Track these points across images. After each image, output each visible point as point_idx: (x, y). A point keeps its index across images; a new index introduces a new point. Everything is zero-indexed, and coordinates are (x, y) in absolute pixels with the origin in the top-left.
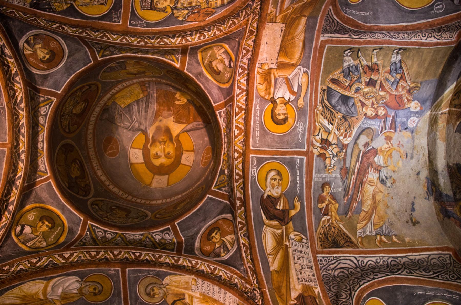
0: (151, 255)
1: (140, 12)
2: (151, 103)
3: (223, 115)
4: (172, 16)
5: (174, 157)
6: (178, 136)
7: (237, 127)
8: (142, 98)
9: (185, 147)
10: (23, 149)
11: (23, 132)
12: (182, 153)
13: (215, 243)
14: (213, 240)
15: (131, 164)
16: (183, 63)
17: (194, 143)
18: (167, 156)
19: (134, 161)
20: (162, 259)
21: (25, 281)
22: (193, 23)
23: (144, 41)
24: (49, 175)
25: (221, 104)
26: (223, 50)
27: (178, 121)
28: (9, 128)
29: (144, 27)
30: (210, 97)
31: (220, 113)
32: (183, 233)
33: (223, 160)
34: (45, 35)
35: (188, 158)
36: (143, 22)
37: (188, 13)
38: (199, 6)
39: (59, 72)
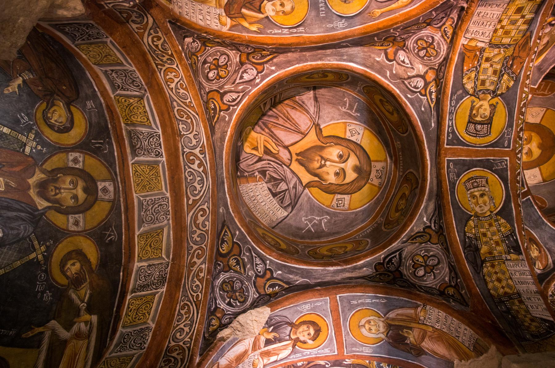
4: (503, 96)
5: (530, 132)
15: (544, 181)
19: (539, 178)
22: (525, 65)
29: (512, 130)
35: (534, 114)
36: (506, 131)
37: (508, 74)
39: (540, 235)
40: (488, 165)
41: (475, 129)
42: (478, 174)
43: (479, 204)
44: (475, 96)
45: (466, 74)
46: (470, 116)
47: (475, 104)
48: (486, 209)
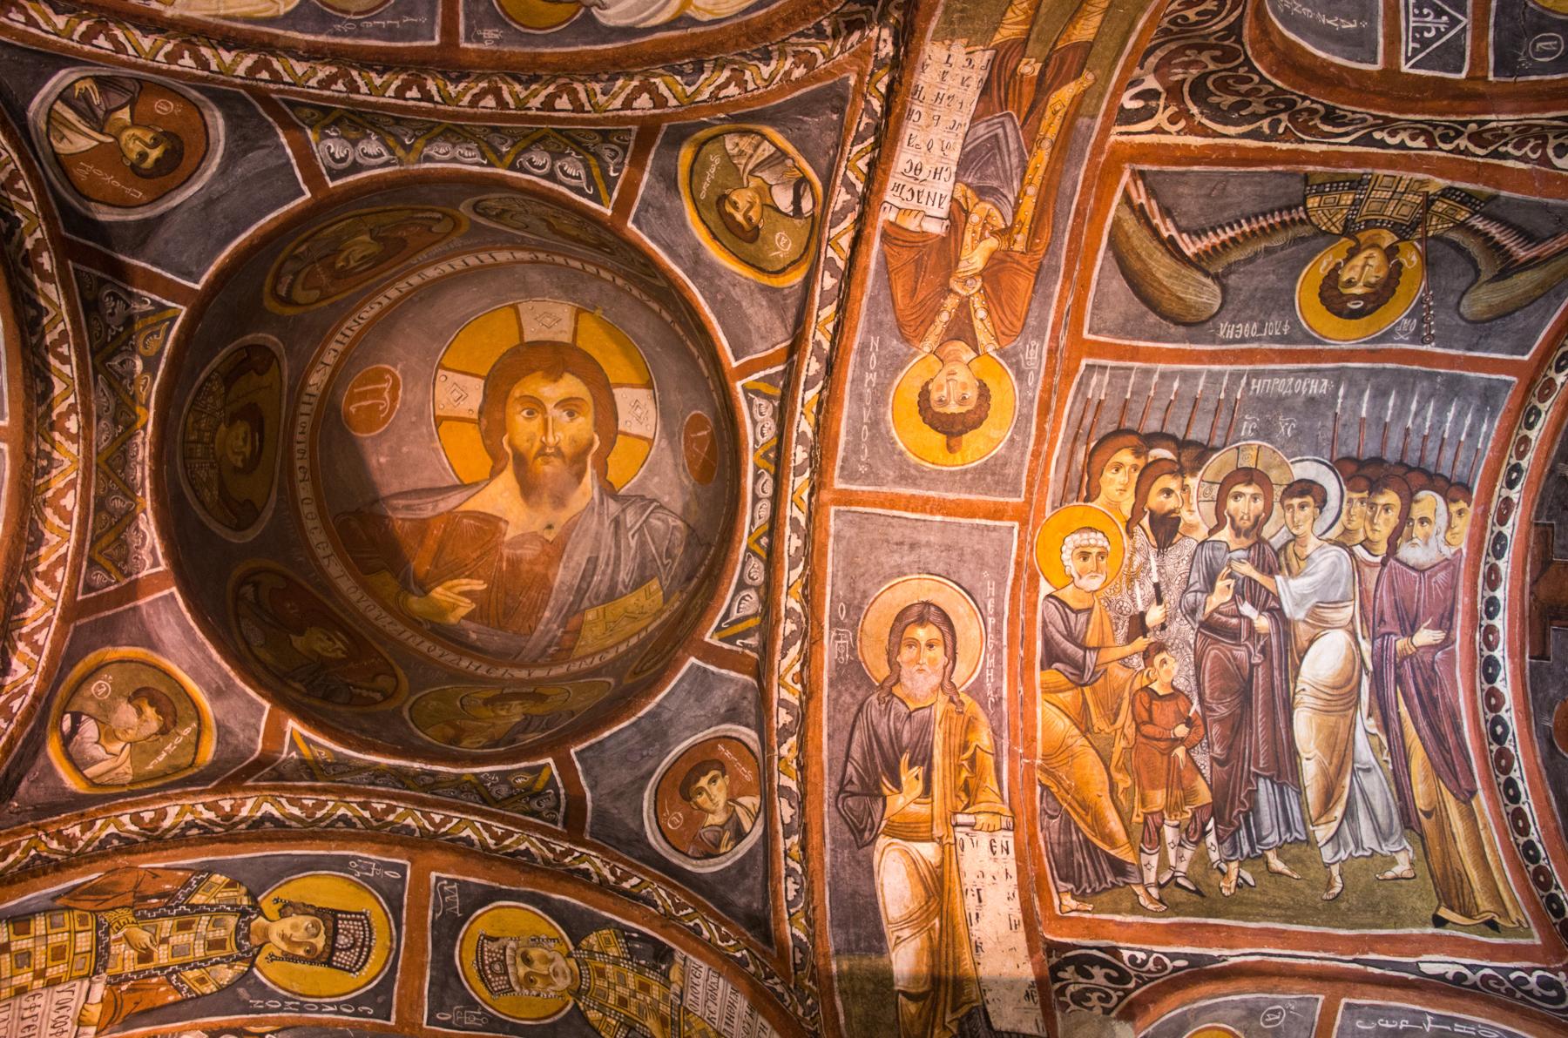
0: (364, 89)
1: (375, 909)
2: (570, 588)
3: (144, 553)
4: (255, 890)
5: (510, 400)
6: (495, 473)
7: (66, 517)
8: (592, 606)
9: (473, 433)
10: (799, 481)
11: (794, 537)
12: (480, 412)
13: (134, 124)
14: (151, 135)
15: (649, 385)
16: (275, 732)
17: (438, 444)
18: (535, 406)
19: (643, 395)
20: (324, 72)
21: (736, 21)
22: (162, 865)
23: (373, 812)
24: (739, 384)
25: (152, 592)
26: (89, 772)
27: (490, 524)
28: (825, 555)
29: (355, 858)
30: (188, 616)
31: (156, 564)
32: (281, 161)
33: (147, 406)
34: (686, 855)
35: (456, 395)
38: (144, 917)
39: (687, 728)
40: (448, 928)
41: (348, 949)
42: (470, 957)
43: (547, 976)
44: (255, 956)
45: (190, 990)
46: (312, 962)
47: (278, 954)
48: (561, 963)
